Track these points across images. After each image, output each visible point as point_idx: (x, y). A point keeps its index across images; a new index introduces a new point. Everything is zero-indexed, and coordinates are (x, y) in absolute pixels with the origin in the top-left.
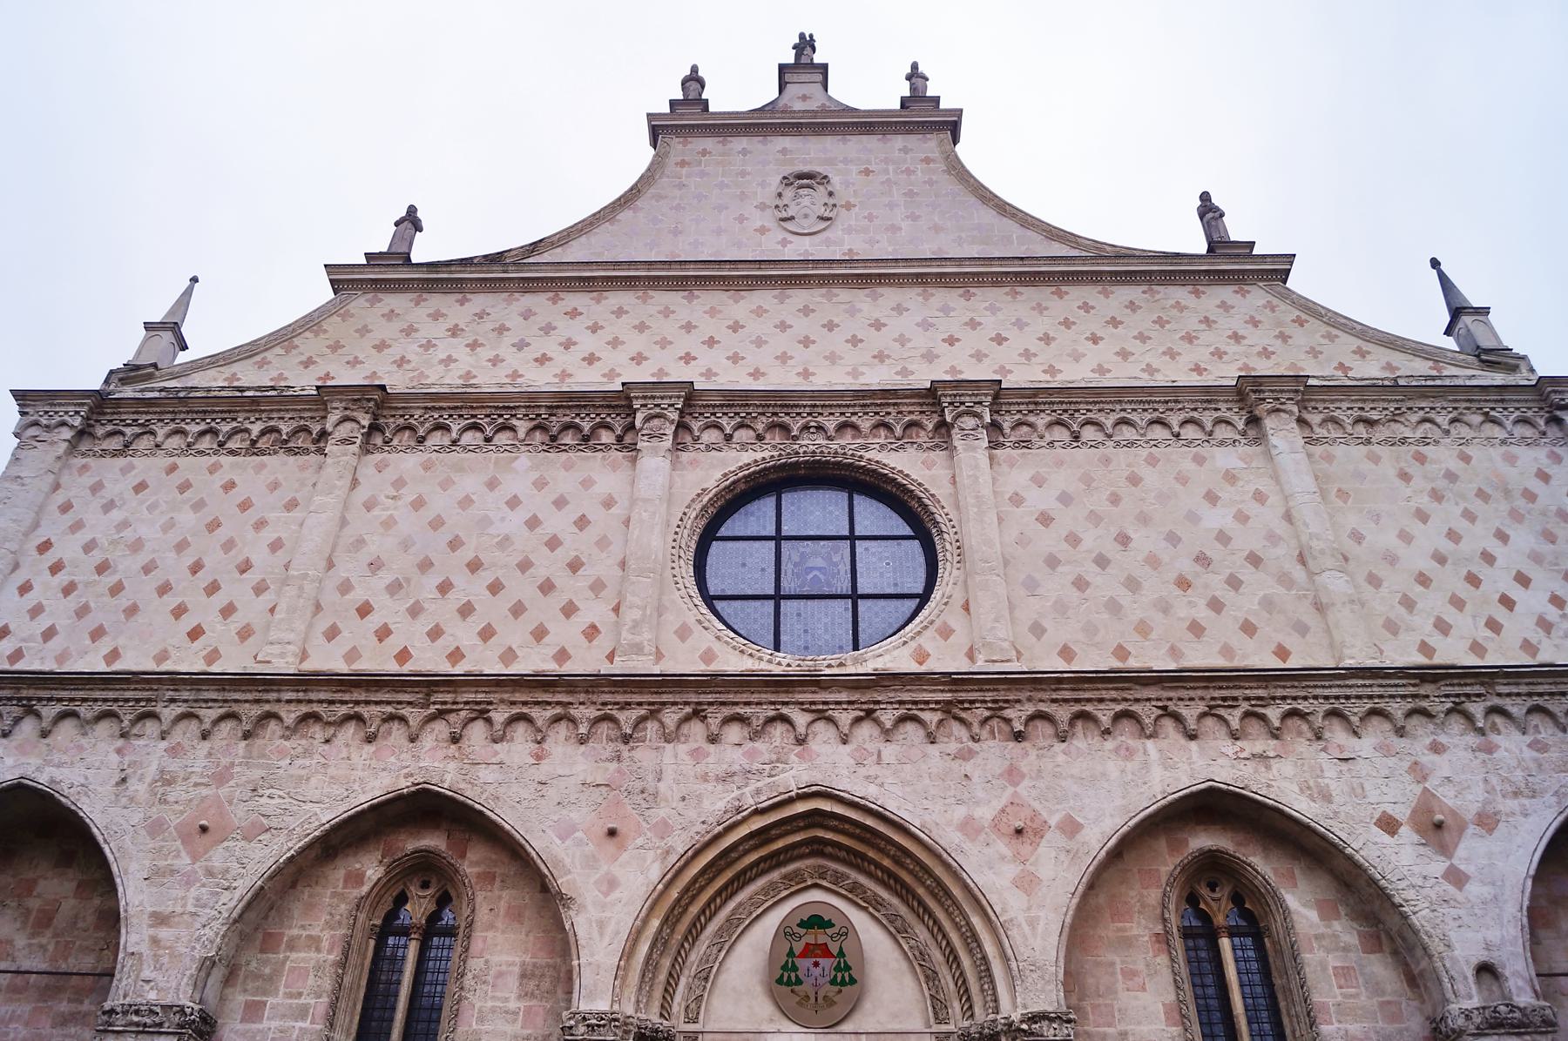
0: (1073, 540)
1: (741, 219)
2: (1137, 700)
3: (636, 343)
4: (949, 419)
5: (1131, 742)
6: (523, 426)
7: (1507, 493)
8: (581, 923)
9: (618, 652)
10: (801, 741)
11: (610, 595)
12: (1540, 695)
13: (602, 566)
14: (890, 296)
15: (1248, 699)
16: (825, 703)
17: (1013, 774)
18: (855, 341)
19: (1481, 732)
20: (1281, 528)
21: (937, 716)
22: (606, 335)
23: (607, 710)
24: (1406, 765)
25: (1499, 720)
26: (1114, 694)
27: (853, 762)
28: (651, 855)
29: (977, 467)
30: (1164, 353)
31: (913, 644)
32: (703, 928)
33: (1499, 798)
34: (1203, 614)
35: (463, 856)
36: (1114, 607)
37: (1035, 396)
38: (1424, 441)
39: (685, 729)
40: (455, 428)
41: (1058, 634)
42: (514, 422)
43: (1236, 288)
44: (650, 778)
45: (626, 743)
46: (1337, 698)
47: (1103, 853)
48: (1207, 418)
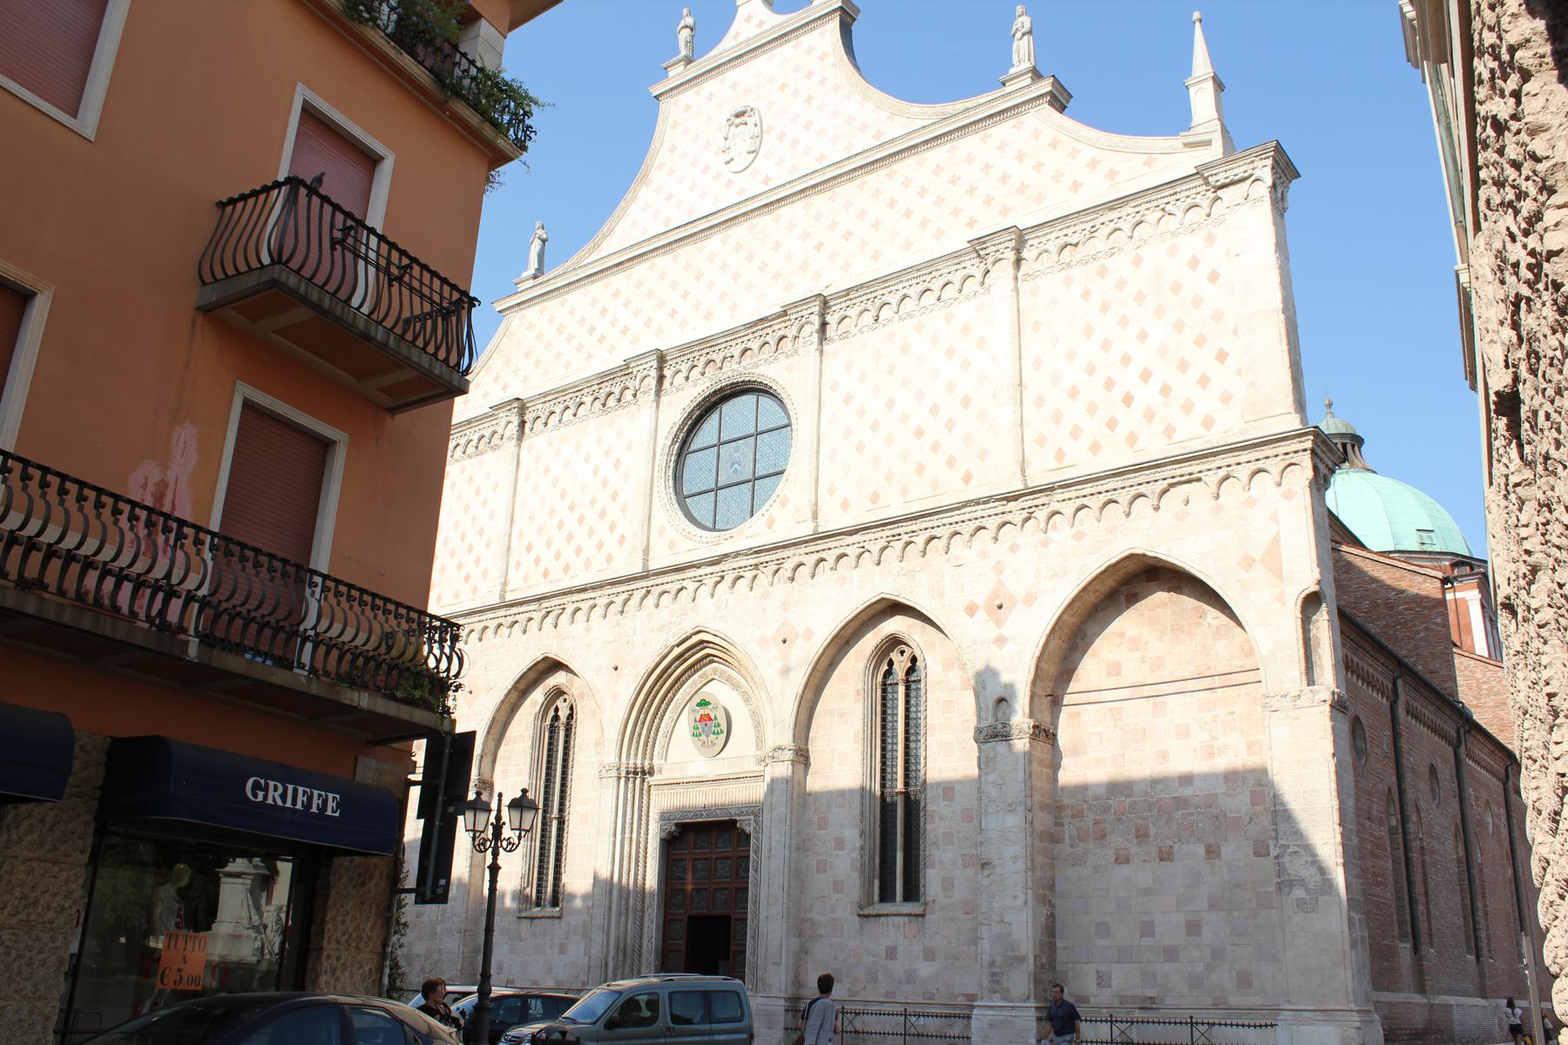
6: (588, 400)
17: (785, 605)
21: (754, 573)
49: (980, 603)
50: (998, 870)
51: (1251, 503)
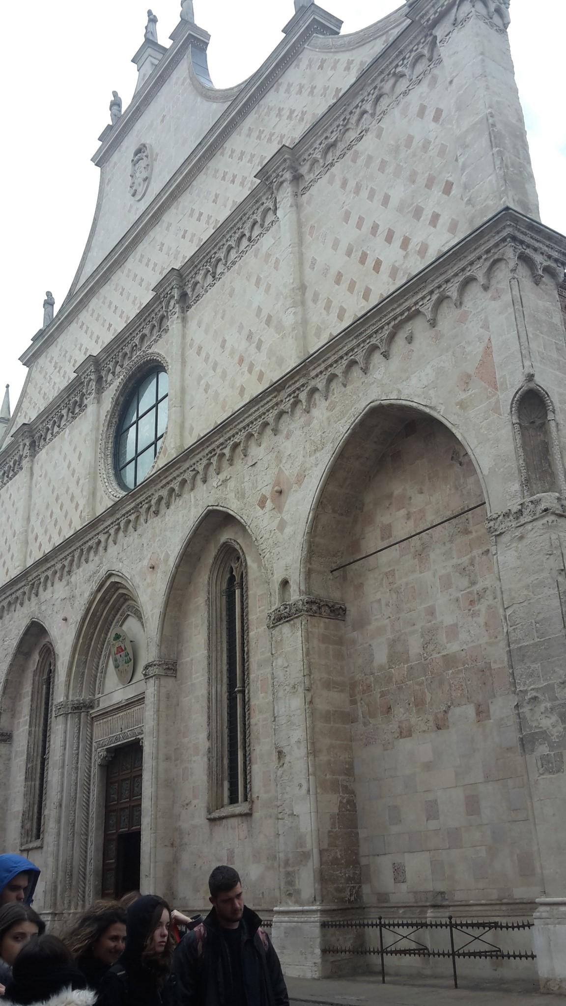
6: (64, 412)
12: (331, 365)
15: (218, 447)
49: (268, 495)
50: (287, 759)
51: (463, 319)
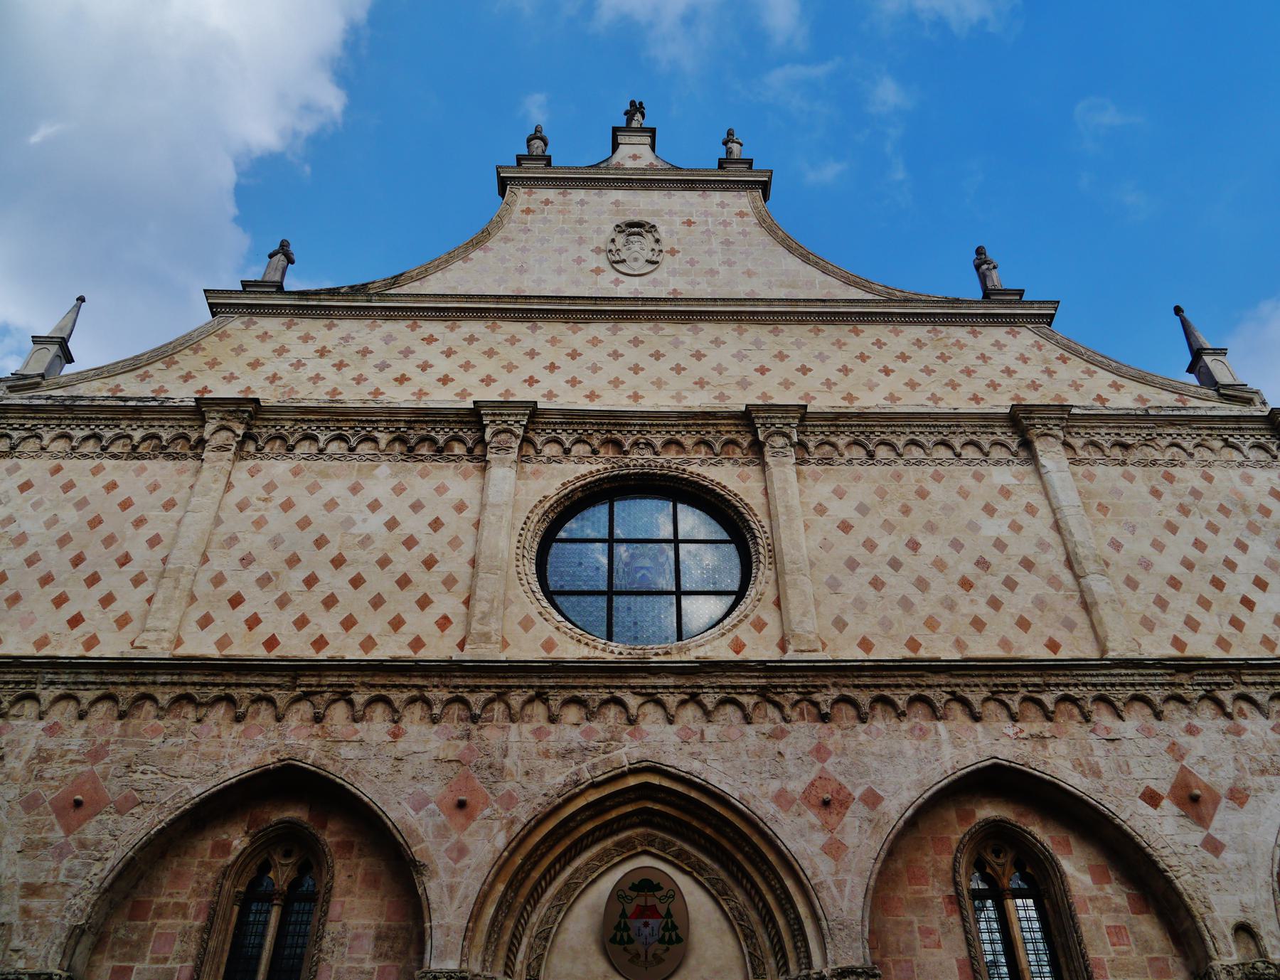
0: (870, 545)
1: (579, 261)
2: (929, 686)
3: (486, 366)
4: (761, 438)
5: (927, 724)
6: (383, 438)
7: (1245, 508)
8: (433, 889)
9: (468, 641)
10: (632, 721)
11: (461, 588)
13: (455, 564)
14: (709, 330)
15: (1025, 685)
16: (655, 687)
18: (678, 369)
19: (1229, 716)
20: (1051, 537)
21: (755, 699)
22: (458, 359)
23: (459, 692)
24: (1165, 745)
25: (1245, 706)
26: (908, 681)
27: (678, 740)
28: (497, 824)
29: (786, 480)
30: (946, 384)
31: (731, 636)
32: (544, 891)
33: (1248, 776)
34: (983, 611)
35: (324, 827)
36: (906, 604)
37: (836, 419)
38: (1172, 463)
39: (528, 710)
40: (322, 438)
41: (859, 627)
42: (376, 434)
43: (1008, 329)
44: (497, 754)
45: (475, 723)
46: (1104, 685)
47: (901, 822)
48: (985, 441)
